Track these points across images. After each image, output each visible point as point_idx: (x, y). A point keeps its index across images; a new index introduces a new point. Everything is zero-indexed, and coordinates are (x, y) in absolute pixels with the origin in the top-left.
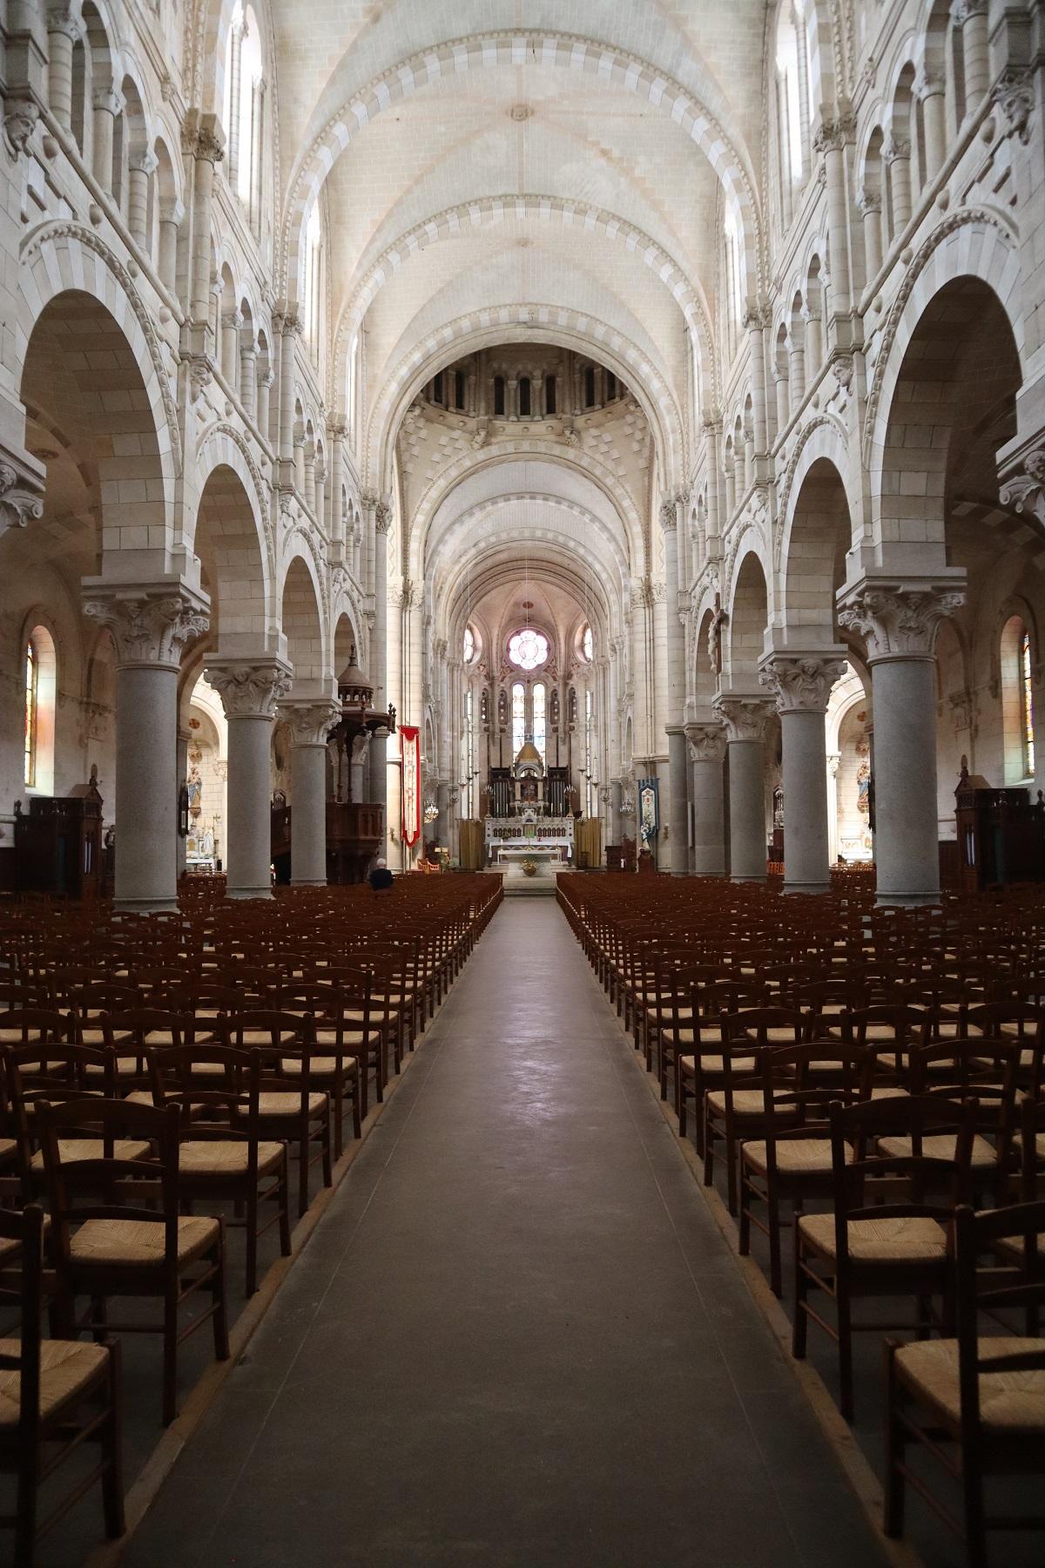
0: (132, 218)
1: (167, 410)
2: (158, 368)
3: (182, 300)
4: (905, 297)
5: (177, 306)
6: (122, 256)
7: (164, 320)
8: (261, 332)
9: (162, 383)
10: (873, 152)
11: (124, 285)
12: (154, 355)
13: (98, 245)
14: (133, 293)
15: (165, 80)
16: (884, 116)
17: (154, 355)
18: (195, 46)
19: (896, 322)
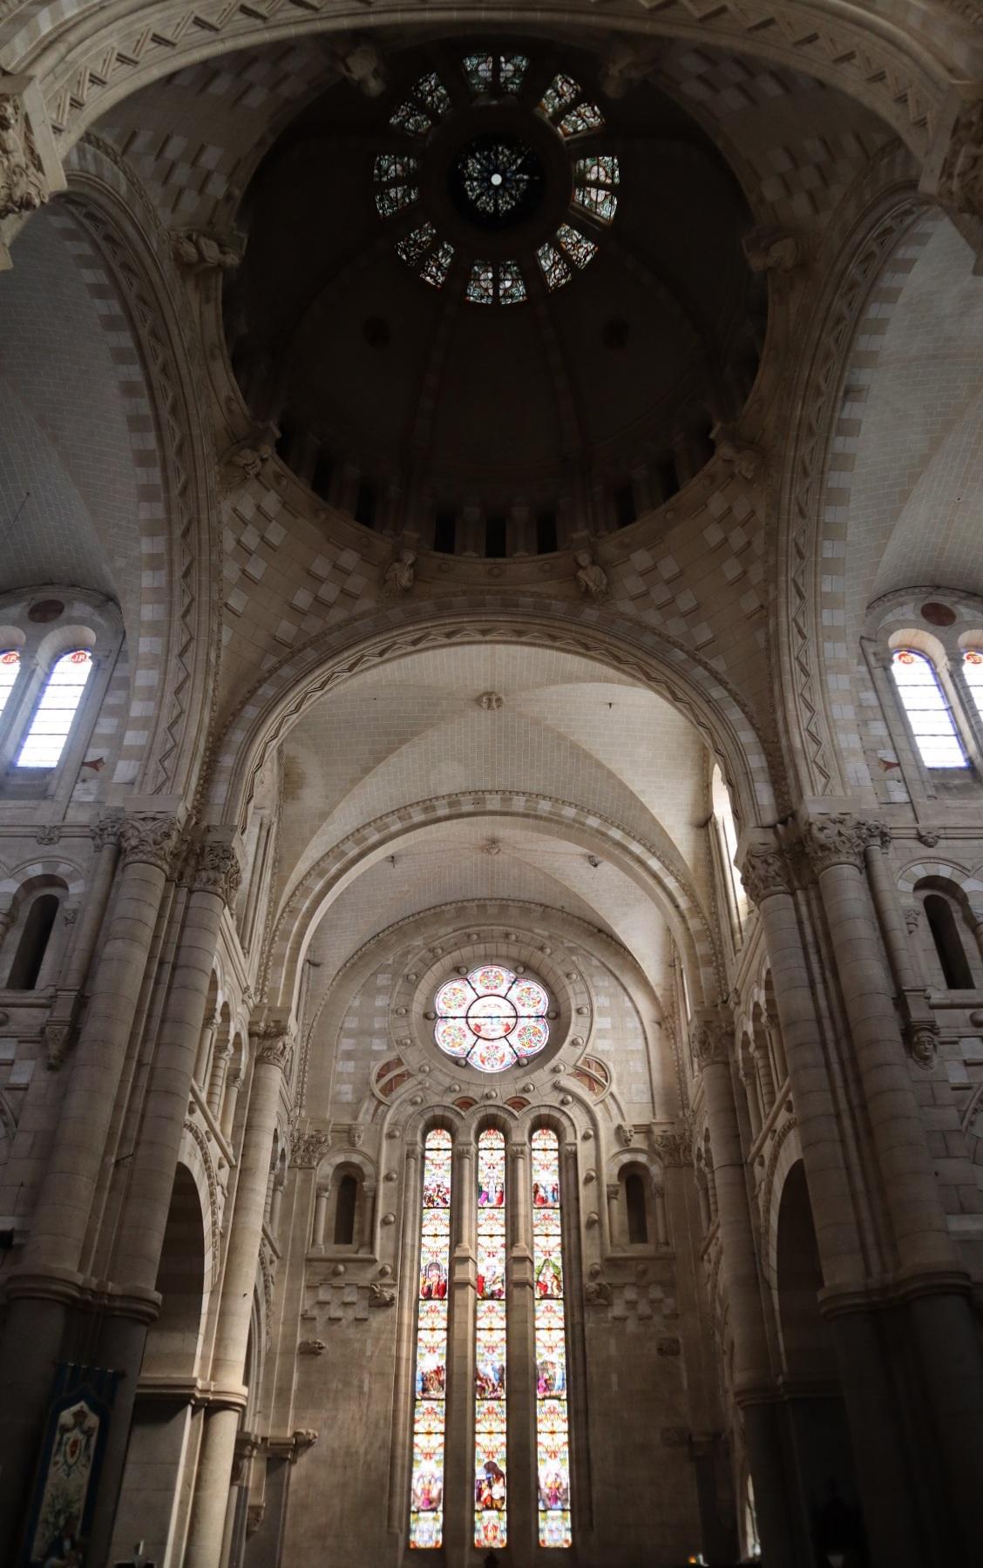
0: (211, 1094)
1: (214, 1234)
2: (213, 1203)
3: (235, 1147)
4: (775, 1158)
5: (230, 1151)
6: (204, 1127)
7: (221, 1166)
8: (283, 1150)
9: (213, 1213)
10: (746, 1044)
11: (202, 1148)
12: (212, 1194)
13: (190, 1126)
14: (206, 1153)
15: (245, 990)
16: (750, 1028)
17: (212, 1194)
18: (267, 963)
19: (772, 1174)
